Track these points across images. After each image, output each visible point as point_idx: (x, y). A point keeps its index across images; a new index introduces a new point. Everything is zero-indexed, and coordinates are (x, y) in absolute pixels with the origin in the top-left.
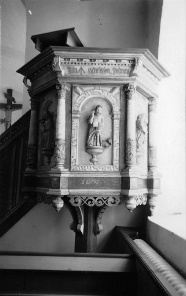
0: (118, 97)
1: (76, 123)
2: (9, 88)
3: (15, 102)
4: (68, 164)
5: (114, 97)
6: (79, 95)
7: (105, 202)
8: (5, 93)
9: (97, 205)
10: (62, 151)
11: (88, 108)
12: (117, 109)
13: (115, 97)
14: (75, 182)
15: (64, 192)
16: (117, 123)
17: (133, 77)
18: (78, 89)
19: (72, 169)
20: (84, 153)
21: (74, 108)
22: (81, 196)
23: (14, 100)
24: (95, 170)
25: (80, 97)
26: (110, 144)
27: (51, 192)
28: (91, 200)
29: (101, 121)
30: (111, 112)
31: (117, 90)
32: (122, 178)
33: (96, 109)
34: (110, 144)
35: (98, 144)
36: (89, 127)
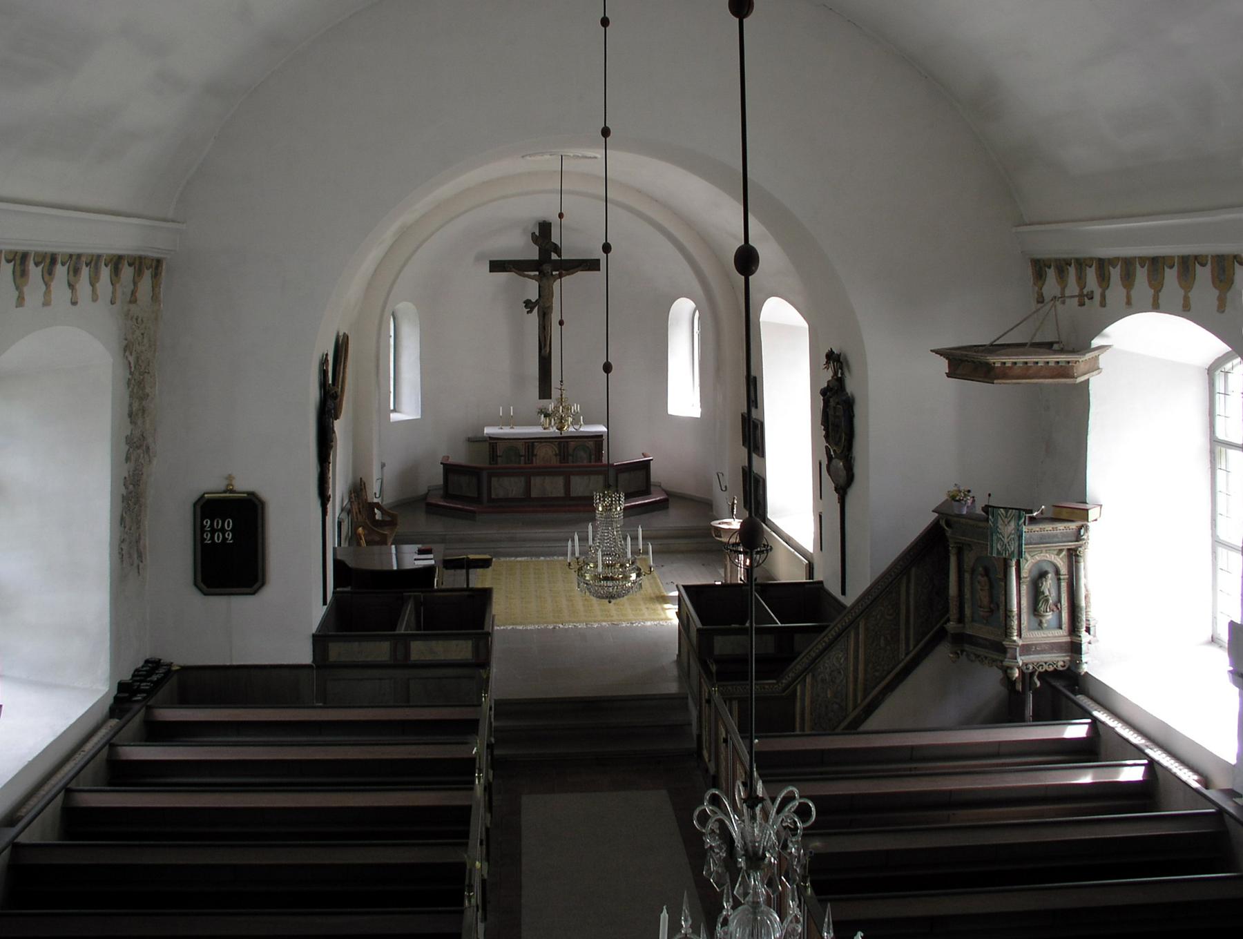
0: (1066, 560)
1: (1024, 588)
2: (541, 220)
4: (1020, 635)
5: (1061, 559)
6: (1027, 561)
7: (1055, 666)
9: (1049, 670)
10: (1015, 623)
11: (1035, 573)
12: (1064, 570)
13: (1061, 562)
16: (1064, 585)
17: (1080, 543)
19: (1023, 636)
20: (1033, 618)
24: (1045, 636)
29: (1048, 586)
32: (1072, 643)
34: (1058, 609)
35: (1048, 610)
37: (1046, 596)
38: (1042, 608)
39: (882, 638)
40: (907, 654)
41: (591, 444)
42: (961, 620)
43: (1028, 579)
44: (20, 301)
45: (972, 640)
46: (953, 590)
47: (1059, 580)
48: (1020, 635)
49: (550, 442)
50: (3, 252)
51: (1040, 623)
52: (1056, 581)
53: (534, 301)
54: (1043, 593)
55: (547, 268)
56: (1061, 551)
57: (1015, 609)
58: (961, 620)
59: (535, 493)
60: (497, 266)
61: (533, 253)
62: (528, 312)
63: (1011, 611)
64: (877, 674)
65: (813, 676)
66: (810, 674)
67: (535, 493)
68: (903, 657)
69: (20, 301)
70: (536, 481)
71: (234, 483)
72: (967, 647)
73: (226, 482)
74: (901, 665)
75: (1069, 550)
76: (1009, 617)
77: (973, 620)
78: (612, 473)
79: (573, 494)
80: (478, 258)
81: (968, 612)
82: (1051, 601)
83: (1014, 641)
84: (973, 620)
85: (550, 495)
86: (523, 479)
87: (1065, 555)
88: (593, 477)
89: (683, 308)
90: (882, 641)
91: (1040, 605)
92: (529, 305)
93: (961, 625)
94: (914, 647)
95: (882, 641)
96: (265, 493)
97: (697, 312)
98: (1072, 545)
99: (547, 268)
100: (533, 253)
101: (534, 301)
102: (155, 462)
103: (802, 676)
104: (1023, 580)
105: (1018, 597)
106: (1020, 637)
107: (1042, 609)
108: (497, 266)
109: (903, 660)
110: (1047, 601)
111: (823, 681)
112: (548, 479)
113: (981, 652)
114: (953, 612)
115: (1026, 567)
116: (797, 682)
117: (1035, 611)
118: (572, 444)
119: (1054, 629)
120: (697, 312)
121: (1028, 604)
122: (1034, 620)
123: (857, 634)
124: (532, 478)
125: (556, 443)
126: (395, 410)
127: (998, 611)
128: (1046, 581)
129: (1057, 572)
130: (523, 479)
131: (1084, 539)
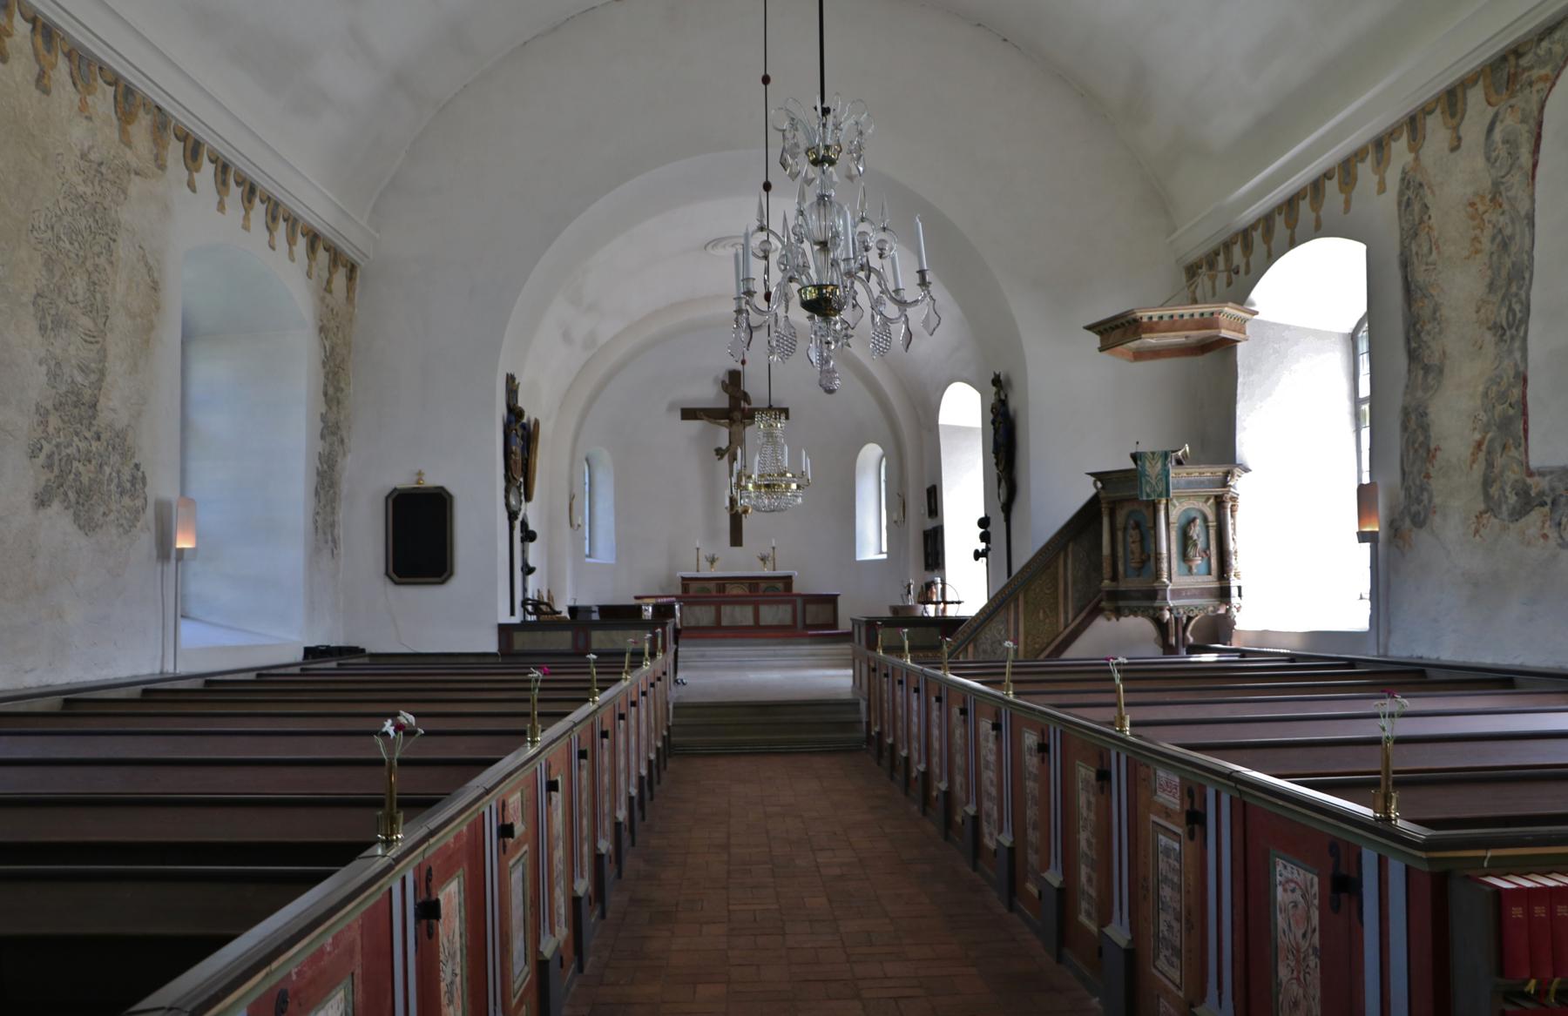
0: (1214, 508)
3: (749, 404)
4: (1170, 578)
5: (1209, 507)
8: (723, 382)
10: (1165, 566)
11: (1184, 521)
12: (1211, 517)
14: (1177, 594)
15: (1171, 603)
16: (1212, 532)
18: (1175, 501)
19: (1173, 581)
20: (1182, 564)
21: (1172, 519)
22: (1183, 607)
23: (746, 397)
25: (1177, 509)
26: (1207, 555)
27: (1158, 604)
28: (1192, 610)
29: (1196, 531)
30: (1205, 519)
31: (1212, 501)
33: (1194, 520)
36: (1186, 540)
37: (1195, 541)
38: (1191, 552)
39: (1041, 611)
40: (1065, 628)
41: (780, 585)
42: (1114, 578)
43: (1177, 525)
44: (221, 207)
45: (1125, 595)
46: (1106, 550)
47: (1207, 527)
48: (1170, 578)
49: (742, 584)
50: (206, 146)
51: (1190, 569)
52: (1204, 529)
53: (724, 447)
54: (1191, 538)
55: (737, 415)
56: (1208, 499)
57: (1164, 550)
58: (1114, 578)
59: (725, 623)
60: (688, 414)
61: (724, 402)
62: (719, 459)
63: (1160, 554)
64: (1037, 646)
65: (975, 646)
66: (972, 645)
67: (725, 623)
68: (1062, 629)
69: (221, 207)
70: (726, 610)
71: (423, 478)
72: (1121, 603)
73: (416, 478)
74: (1060, 638)
75: (1216, 497)
76: (1159, 559)
77: (1126, 576)
78: (799, 602)
79: (762, 623)
80: (671, 408)
81: (1121, 568)
82: (1199, 546)
83: (1164, 582)
84: (1126, 576)
85: (740, 624)
86: (713, 608)
87: (1212, 504)
88: (781, 606)
89: (871, 454)
90: (1041, 615)
91: (1189, 549)
92: (720, 453)
93: (1114, 584)
94: (1073, 620)
95: (1041, 615)
96: (452, 488)
97: (884, 459)
98: (1219, 491)
99: (737, 415)
100: (724, 402)
101: (724, 447)
102: (349, 457)
103: (964, 646)
104: (1171, 525)
105: (1167, 543)
106: (1171, 582)
107: (1191, 554)
108: (688, 414)
109: (1061, 632)
110: (1196, 545)
111: (985, 652)
112: (738, 608)
113: (1134, 603)
114: (1107, 569)
115: (1175, 514)
116: (959, 650)
117: (1185, 557)
118: (763, 585)
119: (1204, 575)
120: (884, 459)
121: (1178, 549)
122: (1184, 567)
123: (1017, 607)
124: (723, 608)
125: (747, 585)
126: (590, 556)
127: (1149, 560)
128: (1194, 526)
129: (1205, 519)
130: (713, 608)
131: (1230, 486)
